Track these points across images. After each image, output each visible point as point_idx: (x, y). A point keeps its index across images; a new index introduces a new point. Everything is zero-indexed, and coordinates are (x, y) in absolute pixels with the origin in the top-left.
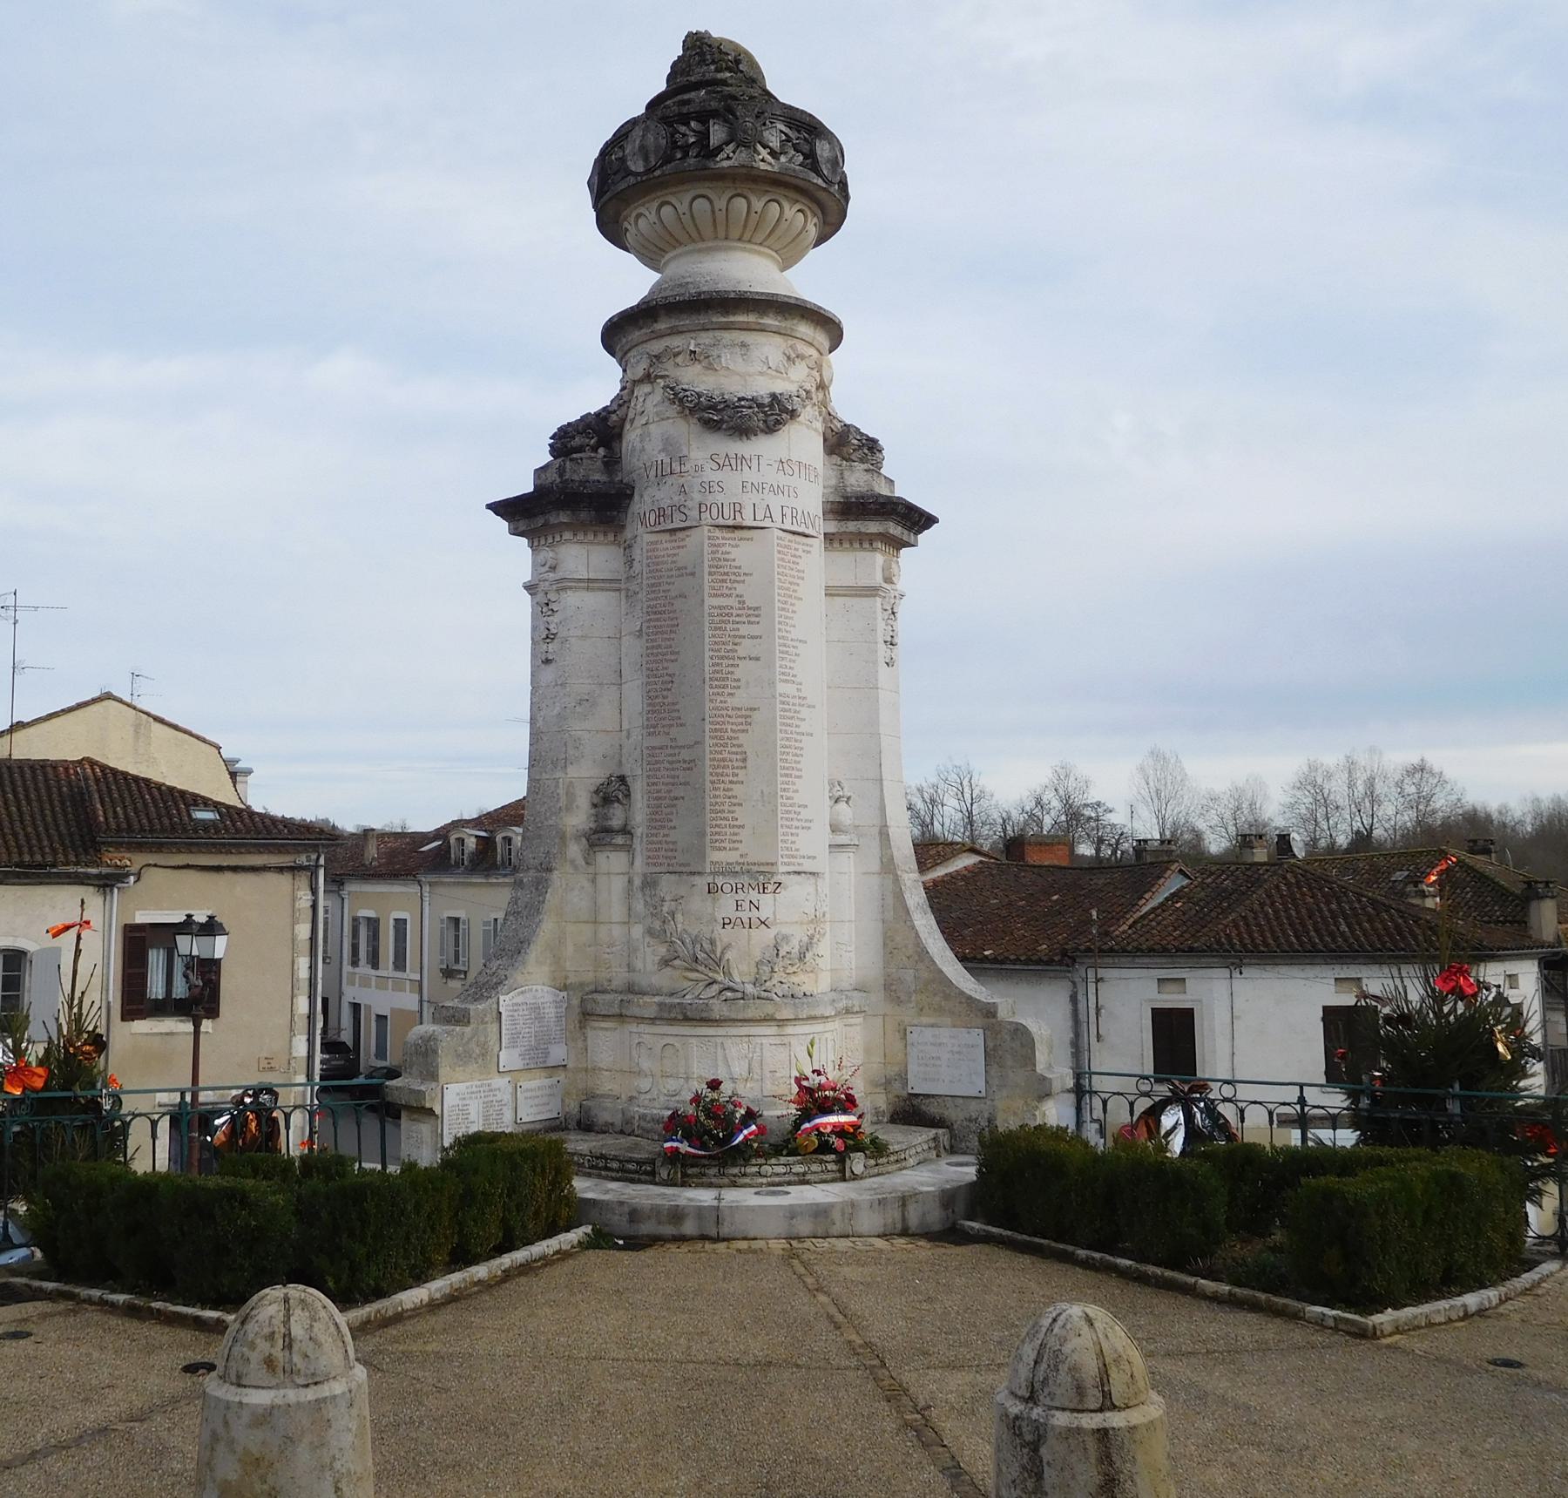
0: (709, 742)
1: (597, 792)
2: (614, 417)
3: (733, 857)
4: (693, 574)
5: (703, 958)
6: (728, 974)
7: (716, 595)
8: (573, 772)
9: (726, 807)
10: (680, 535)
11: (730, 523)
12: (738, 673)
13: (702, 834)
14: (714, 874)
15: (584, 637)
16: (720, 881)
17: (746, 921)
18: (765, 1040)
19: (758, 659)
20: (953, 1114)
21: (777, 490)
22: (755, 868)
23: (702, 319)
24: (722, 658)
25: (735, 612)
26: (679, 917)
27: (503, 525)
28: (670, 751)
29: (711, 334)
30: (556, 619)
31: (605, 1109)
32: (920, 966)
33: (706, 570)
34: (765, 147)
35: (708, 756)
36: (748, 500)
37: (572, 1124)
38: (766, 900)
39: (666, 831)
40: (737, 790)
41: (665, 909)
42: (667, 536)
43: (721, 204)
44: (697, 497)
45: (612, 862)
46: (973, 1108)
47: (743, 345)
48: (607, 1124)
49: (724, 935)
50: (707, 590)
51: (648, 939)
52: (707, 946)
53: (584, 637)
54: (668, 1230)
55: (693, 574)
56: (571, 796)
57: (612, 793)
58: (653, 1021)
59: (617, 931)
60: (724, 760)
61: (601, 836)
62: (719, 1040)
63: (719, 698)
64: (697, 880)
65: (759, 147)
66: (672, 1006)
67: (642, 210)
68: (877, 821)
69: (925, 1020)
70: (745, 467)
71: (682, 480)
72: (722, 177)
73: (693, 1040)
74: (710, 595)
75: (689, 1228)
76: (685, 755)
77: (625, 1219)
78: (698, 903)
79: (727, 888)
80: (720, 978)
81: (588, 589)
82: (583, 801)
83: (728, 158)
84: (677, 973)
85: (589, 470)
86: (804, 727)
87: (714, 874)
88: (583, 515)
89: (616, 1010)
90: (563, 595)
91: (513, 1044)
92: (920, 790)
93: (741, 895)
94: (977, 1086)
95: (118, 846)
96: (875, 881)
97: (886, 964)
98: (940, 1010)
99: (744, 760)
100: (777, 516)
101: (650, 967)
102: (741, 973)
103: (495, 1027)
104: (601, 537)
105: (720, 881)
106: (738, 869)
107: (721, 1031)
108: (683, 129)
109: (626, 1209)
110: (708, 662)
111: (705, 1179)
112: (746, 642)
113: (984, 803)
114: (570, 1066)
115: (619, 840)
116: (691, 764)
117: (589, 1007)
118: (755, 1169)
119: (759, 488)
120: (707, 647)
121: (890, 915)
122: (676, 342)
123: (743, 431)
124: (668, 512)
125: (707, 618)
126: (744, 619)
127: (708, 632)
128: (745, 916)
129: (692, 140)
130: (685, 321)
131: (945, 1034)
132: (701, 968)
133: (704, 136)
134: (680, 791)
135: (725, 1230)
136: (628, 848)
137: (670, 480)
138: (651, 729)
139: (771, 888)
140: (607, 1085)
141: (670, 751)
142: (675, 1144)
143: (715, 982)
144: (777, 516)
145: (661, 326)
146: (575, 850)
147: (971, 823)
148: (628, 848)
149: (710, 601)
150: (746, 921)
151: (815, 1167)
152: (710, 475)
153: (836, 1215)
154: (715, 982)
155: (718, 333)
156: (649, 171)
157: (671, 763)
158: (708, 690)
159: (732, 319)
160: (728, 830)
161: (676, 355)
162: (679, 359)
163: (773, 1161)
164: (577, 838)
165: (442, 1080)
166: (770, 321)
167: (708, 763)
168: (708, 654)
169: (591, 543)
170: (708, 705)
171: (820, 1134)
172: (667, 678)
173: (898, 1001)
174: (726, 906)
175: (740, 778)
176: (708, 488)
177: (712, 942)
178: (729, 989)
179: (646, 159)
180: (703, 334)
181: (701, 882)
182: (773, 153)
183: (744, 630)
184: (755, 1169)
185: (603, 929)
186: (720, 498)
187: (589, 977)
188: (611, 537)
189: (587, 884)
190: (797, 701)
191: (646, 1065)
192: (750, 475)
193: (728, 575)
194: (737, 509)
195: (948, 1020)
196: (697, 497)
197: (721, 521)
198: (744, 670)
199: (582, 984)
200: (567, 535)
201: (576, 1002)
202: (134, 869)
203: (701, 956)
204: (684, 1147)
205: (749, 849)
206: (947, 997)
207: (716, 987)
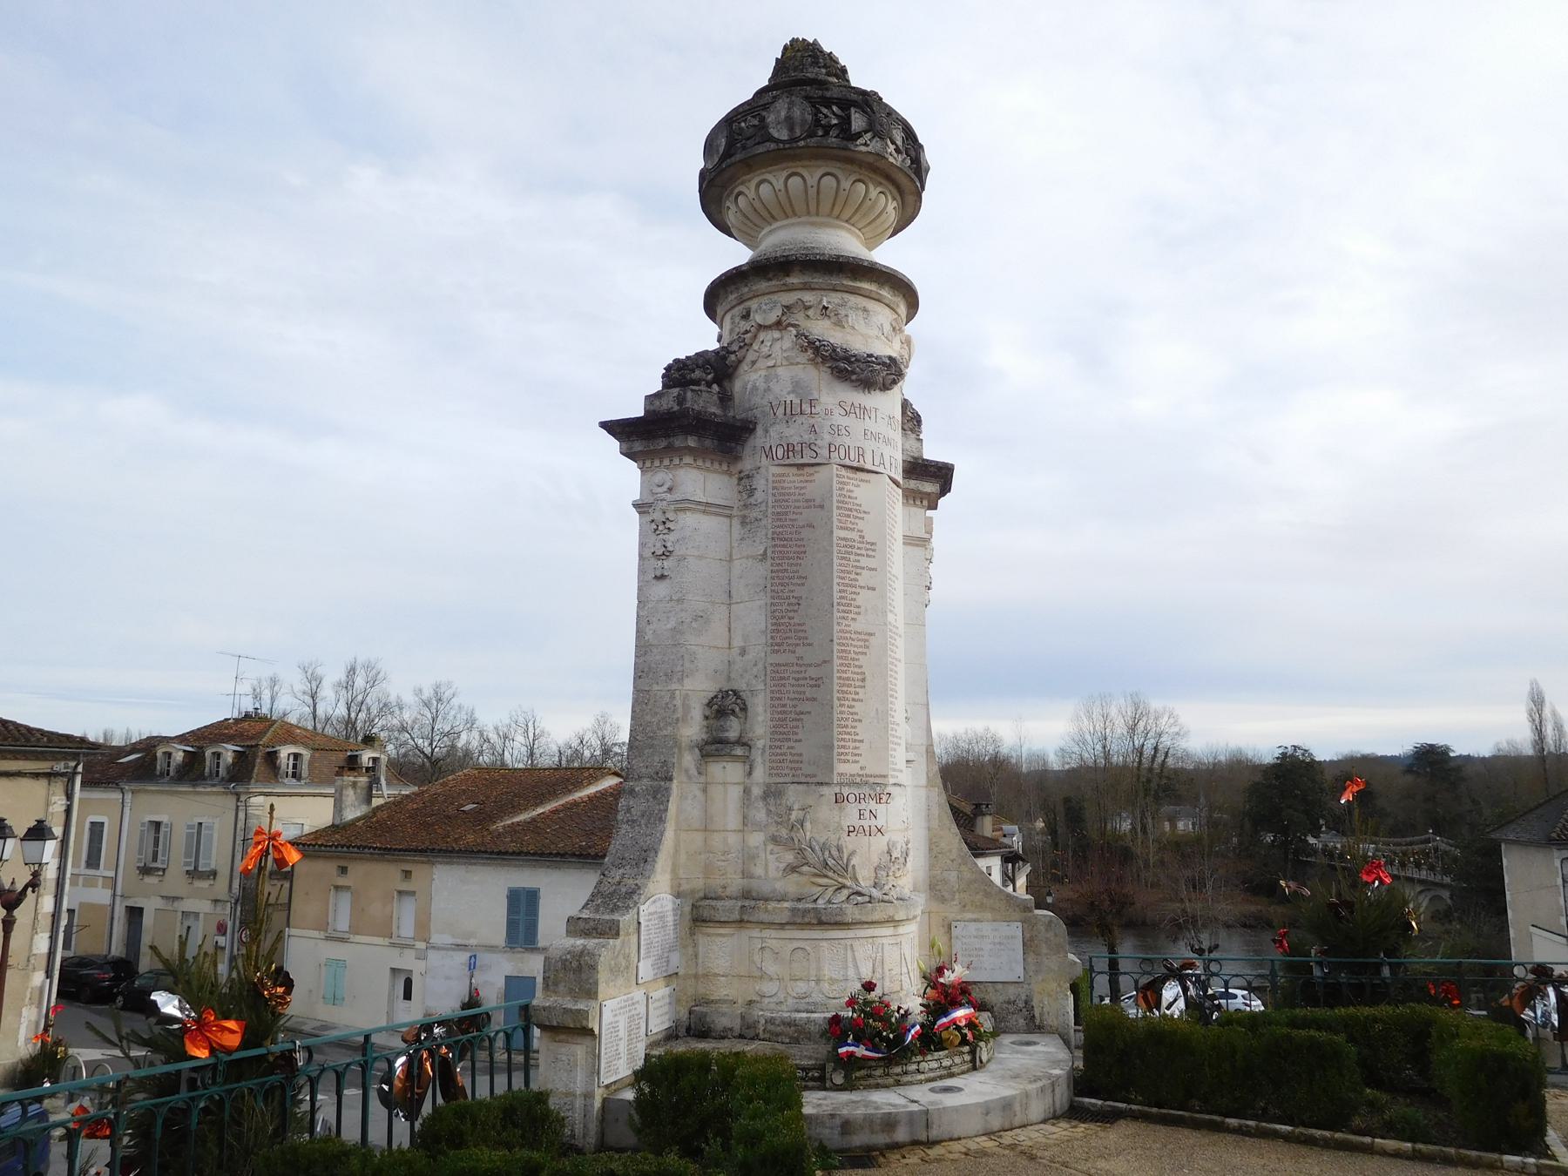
0: (837, 662)
1: (709, 704)
2: (733, 357)
5: (830, 865)
6: (855, 879)
8: (689, 684)
9: (849, 723)
11: (855, 464)
12: (860, 600)
13: (831, 747)
14: (841, 784)
15: (700, 557)
16: (846, 791)
18: (885, 941)
20: (993, 998)
22: (872, 780)
23: (835, 281)
26: (808, 825)
27: (613, 444)
28: (796, 668)
29: (839, 295)
30: (671, 537)
31: (724, 1014)
32: (963, 868)
34: (893, 143)
35: (836, 675)
36: (869, 446)
37: (682, 1032)
38: (880, 809)
39: (791, 744)
40: (858, 707)
41: (793, 817)
42: (794, 470)
43: (846, 184)
44: (827, 438)
45: (727, 772)
46: (1012, 992)
47: (865, 310)
48: (725, 1029)
49: (849, 843)
50: (836, 523)
51: (770, 847)
52: (835, 853)
53: (700, 557)
54: (881, 1139)
55: (822, 507)
56: (687, 708)
57: (725, 706)
58: (782, 926)
59: (733, 839)
61: (715, 747)
62: (849, 942)
64: (825, 790)
66: (807, 911)
67: (769, 177)
68: (924, 741)
69: (969, 916)
71: (812, 421)
72: (851, 161)
73: (824, 944)
75: (901, 1135)
76: (812, 672)
77: (837, 1131)
78: (825, 811)
80: (848, 883)
81: (704, 512)
82: (697, 713)
83: (866, 144)
84: (804, 879)
85: (704, 401)
87: (841, 784)
88: (708, 443)
89: (736, 916)
90: (681, 516)
92: (496, 728)
93: (863, 805)
94: (1017, 972)
96: (923, 792)
97: (931, 867)
98: (981, 907)
99: (863, 680)
101: (772, 873)
102: (865, 880)
103: (634, 939)
104: (716, 465)
105: (846, 791)
107: (851, 934)
108: (825, 111)
109: (838, 1121)
110: (836, 588)
111: (872, 1081)
112: (864, 572)
113: (543, 740)
114: (681, 972)
115: (739, 751)
116: (817, 683)
117: (699, 914)
118: (914, 1067)
119: (876, 437)
121: (935, 824)
122: (808, 297)
123: (867, 385)
124: (798, 448)
125: (835, 549)
128: (866, 824)
129: (835, 121)
130: (818, 280)
131: (986, 928)
132: (830, 874)
133: (846, 121)
134: (807, 706)
135: (934, 1133)
136: (747, 760)
137: (800, 419)
138: (776, 647)
139: (884, 798)
140: (722, 990)
141: (796, 668)
142: (851, 1049)
143: (844, 886)
145: (794, 280)
146: (689, 760)
147: (532, 754)
148: (747, 760)
149: (838, 533)
151: (957, 1060)
152: (839, 419)
153: (1017, 1107)
154: (844, 886)
155: (846, 296)
156: (793, 140)
158: (836, 614)
159: (858, 284)
160: (852, 745)
161: (807, 308)
162: (810, 313)
163: (929, 1057)
164: (691, 748)
165: (600, 996)
166: (886, 293)
167: (836, 681)
168: (836, 580)
169: (707, 469)
170: (836, 628)
171: (958, 1028)
173: (943, 900)
174: (850, 815)
175: (861, 696)
176: (836, 430)
177: (839, 849)
178: (859, 894)
179: (791, 129)
180: (833, 294)
181: (829, 792)
183: (864, 562)
184: (914, 1067)
186: (847, 441)
187: (699, 884)
188: (725, 467)
189: (699, 794)
191: (771, 968)
192: (869, 424)
193: (854, 512)
194: (861, 455)
195: (989, 915)
196: (827, 438)
197: (847, 462)
198: (863, 598)
199: (693, 892)
200: (688, 460)
201: (687, 909)
203: (831, 862)
204: (861, 1051)
205: (867, 763)
206: (987, 895)
207: (845, 892)
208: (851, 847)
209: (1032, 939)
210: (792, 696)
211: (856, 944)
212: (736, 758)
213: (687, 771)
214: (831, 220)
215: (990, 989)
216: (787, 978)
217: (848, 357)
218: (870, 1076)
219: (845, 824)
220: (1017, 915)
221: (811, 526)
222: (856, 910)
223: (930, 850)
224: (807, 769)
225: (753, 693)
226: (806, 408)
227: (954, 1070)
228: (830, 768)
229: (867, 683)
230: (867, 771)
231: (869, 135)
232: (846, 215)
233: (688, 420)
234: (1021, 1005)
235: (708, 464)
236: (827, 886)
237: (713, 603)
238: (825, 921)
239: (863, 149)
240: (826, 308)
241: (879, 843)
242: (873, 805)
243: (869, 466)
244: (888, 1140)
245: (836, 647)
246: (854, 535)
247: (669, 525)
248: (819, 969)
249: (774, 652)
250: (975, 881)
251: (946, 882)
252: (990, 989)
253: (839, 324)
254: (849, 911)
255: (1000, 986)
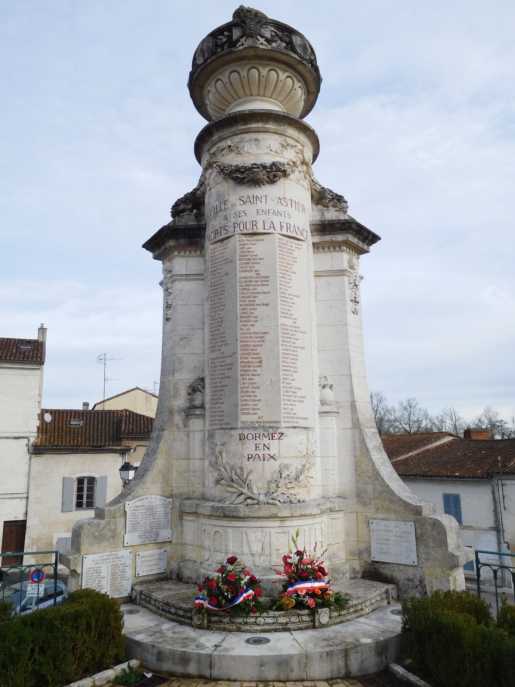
0: (239, 352)
1: (190, 387)
2: (199, 192)
3: (254, 418)
4: (231, 261)
5: (236, 480)
6: (249, 488)
7: (243, 271)
8: (177, 376)
9: (250, 390)
10: (226, 242)
11: (250, 231)
12: (256, 313)
13: (236, 405)
14: (243, 428)
15: (184, 305)
16: (246, 432)
17: (261, 456)
18: (272, 530)
19: (268, 305)
20: (399, 575)
21: (277, 213)
22: (268, 425)
23: (234, 129)
24: (247, 305)
25: (254, 280)
26: (224, 455)
27: (150, 254)
28: (221, 360)
29: (239, 136)
30: (171, 297)
31: (188, 569)
32: (376, 483)
33: (238, 258)
34: (262, 37)
35: (239, 360)
36: (260, 219)
37: (174, 576)
38: (274, 445)
39: (219, 405)
40: (256, 379)
41: (217, 450)
42: (219, 244)
43: (244, 73)
44: (233, 220)
45: (196, 424)
46: (411, 572)
47: (256, 140)
48: (189, 578)
49: (248, 465)
50: (238, 269)
51: (210, 468)
52: (239, 472)
53: (184, 305)
54: (179, 669)
55: (231, 261)
56: (176, 390)
57: (196, 387)
58: (210, 516)
59: (197, 463)
60: (249, 362)
61: (192, 410)
62: (244, 530)
63: (245, 328)
64: (233, 432)
65: (259, 37)
66: (218, 508)
67: (209, 88)
68: (349, 399)
69: (380, 516)
70: (258, 202)
71: (225, 213)
72: (242, 59)
73: (230, 530)
74: (240, 271)
75: (192, 669)
76: (228, 361)
77: (155, 657)
78: (234, 446)
79: (250, 437)
80: (245, 491)
81: (186, 280)
82: (183, 392)
83: (243, 45)
84: (223, 488)
85: (188, 220)
86: (298, 344)
87: (243, 428)
88: (182, 241)
89: (193, 510)
90: (174, 284)
91: (134, 529)
92: (437, 418)
93: (258, 441)
94: (412, 558)
95: (128, 439)
96: (349, 433)
97: (357, 481)
98: (388, 510)
99: (260, 362)
100: (278, 227)
101: (212, 485)
102: (258, 488)
103: (122, 520)
104: (193, 253)
105: (246, 432)
106: (257, 425)
107: (245, 524)
108: (220, 37)
109: (155, 651)
110: (239, 307)
111: (222, 626)
112: (260, 296)
113: (460, 421)
114: (174, 541)
115: (198, 412)
116: (231, 366)
117: (184, 507)
118: (253, 620)
119: (267, 212)
120: (238, 300)
121: (358, 453)
122: (223, 144)
123: (256, 182)
124: (219, 231)
125: (238, 284)
126: (259, 283)
127: (239, 291)
128: (260, 453)
129: (224, 40)
130: (226, 132)
131: (392, 525)
132: (235, 485)
133: (230, 37)
134: (225, 382)
135: (216, 673)
136: (203, 416)
137: (220, 214)
138: (213, 349)
139: (277, 436)
140: (191, 554)
141: (221, 360)
142: (201, 601)
143: (242, 494)
144: (278, 227)
145: (215, 138)
146: (178, 419)
147: (456, 428)
148: (203, 416)
149: (240, 275)
150: (261, 456)
151: (294, 619)
152: (240, 208)
153: (295, 665)
154: (242, 494)
155: (243, 136)
156: (205, 61)
157: (221, 366)
158: (239, 324)
159: (249, 126)
161: (222, 150)
162: (224, 152)
163: (265, 615)
164: (179, 412)
165: (83, 552)
166: (271, 126)
167: (239, 364)
168: (239, 303)
169: (188, 256)
170: (239, 332)
171: (298, 596)
172: (220, 320)
173: (364, 504)
174: (250, 448)
175: (258, 373)
176: (238, 215)
177: (242, 469)
178: (250, 498)
179: (204, 56)
180: (235, 137)
181: (235, 433)
182: (267, 40)
183: (260, 289)
184: (253, 620)
185: (191, 462)
186: (244, 219)
187: (184, 490)
188: (198, 253)
189: (184, 438)
190: (293, 329)
191: (207, 543)
192: (261, 206)
193: (250, 260)
194: (254, 224)
195: (393, 516)
196: (233, 220)
197: (245, 231)
198: (259, 311)
199: (181, 494)
200: (176, 253)
201: (177, 504)
202: (133, 447)
203: (235, 477)
204: (206, 604)
205: (265, 414)
206: (392, 502)
207: (243, 497)
208: (250, 468)
209: (422, 535)
210: (220, 376)
211: (250, 531)
212: (198, 416)
213: (177, 425)
214: (248, 98)
215: (396, 568)
216: (212, 549)
217: (238, 169)
218: (221, 622)
219: (246, 453)
220: (412, 517)
221: (227, 274)
222: (246, 509)
223: (356, 470)
224: (226, 420)
225: (212, 379)
226: (223, 207)
227: (289, 626)
228: (236, 418)
229: (263, 364)
230: (264, 419)
231: (244, 39)
232: (269, 93)
233: (184, 232)
234: (417, 583)
235: (188, 253)
236: (233, 493)
237: (193, 329)
238: (228, 515)
239: (241, 48)
240: (230, 146)
241: (272, 466)
242: (266, 441)
243: (261, 230)
244: (183, 671)
245: (239, 344)
246: (253, 274)
247: (170, 291)
248: (227, 546)
249: (212, 351)
250: (383, 492)
251: (365, 491)
252: (396, 568)
253: (239, 153)
254: (241, 510)
255: (402, 568)
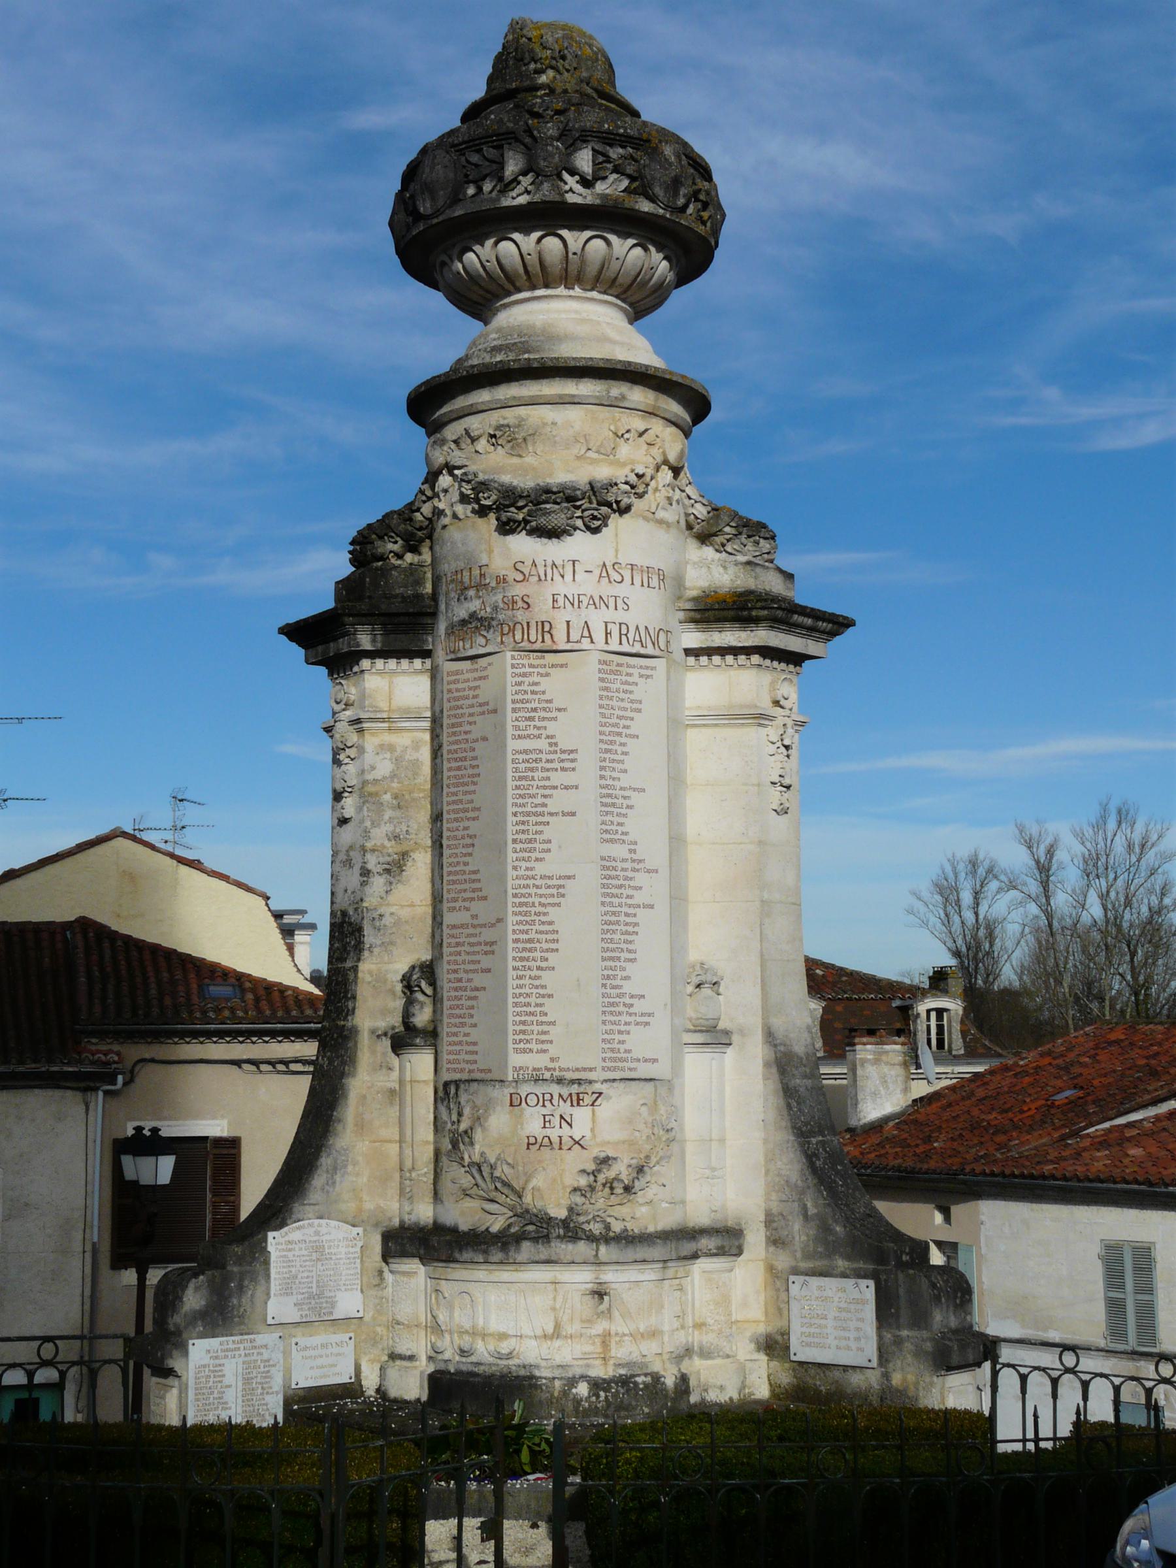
0: (511, 919)
3: (540, 1061)
4: (495, 711)
7: (520, 737)
10: (482, 662)
12: (548, 832)
16: (524, 1090)
17: (555, 1140)
19: (573, 814)
21: (597, 602)
24: (528, 814)
25: (544, 757)
28: (471, 931)
33: (510, 706)
34: (572, 174)
35: (511, 937)
36: (559, 619)
39: (467, 1030)
50: (510, 731)
55: (495, 711)
60: (530, 941)
63: (524, 864)
65: (566, 176)
70: (557, 577)
74: (514, 737)
79: (532, 1100)
86: (639, 898)
95: (102, 1035)
100: (599, 636)
106: (547, 1075)
108: (475, 158)
110: (511, 819)
119: (575, 602)
120: (510, 801)
126: (556, 765)
127: (510, 784)
128: (554, 1134)
139: (588, 1100)
141: (471, 931)
144: (599, 636)
149: (512, 745)
150: (555, 1140)
157: (471, 944)
160: (535, 1028)
168: (511, 810)
170: (511, 873)
172: (468, 841)
175: (550, 964)
183: (557, 778)
190: (628, 865)
194: (545, 628)
197: (525, 645)
202: (129, 1064)
230: (562, 1064)
242: (565, 1108)
246: (542, 744)
